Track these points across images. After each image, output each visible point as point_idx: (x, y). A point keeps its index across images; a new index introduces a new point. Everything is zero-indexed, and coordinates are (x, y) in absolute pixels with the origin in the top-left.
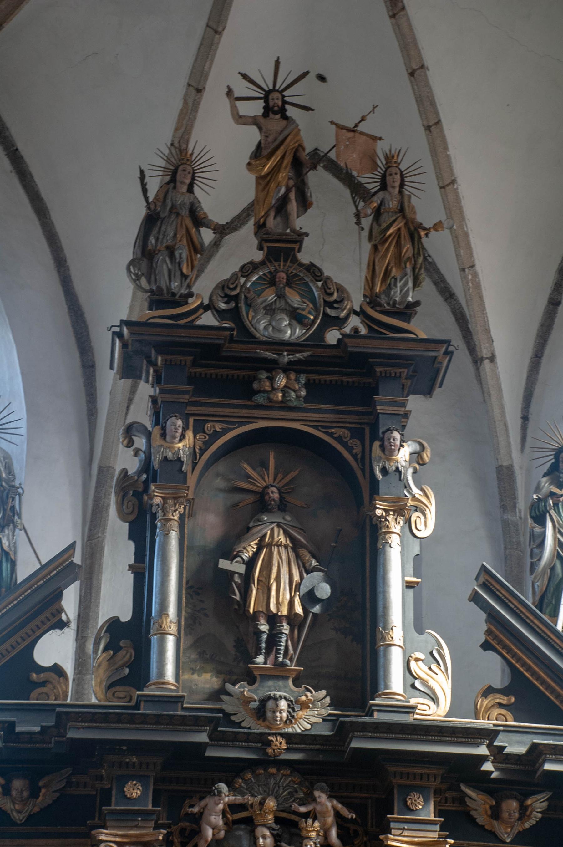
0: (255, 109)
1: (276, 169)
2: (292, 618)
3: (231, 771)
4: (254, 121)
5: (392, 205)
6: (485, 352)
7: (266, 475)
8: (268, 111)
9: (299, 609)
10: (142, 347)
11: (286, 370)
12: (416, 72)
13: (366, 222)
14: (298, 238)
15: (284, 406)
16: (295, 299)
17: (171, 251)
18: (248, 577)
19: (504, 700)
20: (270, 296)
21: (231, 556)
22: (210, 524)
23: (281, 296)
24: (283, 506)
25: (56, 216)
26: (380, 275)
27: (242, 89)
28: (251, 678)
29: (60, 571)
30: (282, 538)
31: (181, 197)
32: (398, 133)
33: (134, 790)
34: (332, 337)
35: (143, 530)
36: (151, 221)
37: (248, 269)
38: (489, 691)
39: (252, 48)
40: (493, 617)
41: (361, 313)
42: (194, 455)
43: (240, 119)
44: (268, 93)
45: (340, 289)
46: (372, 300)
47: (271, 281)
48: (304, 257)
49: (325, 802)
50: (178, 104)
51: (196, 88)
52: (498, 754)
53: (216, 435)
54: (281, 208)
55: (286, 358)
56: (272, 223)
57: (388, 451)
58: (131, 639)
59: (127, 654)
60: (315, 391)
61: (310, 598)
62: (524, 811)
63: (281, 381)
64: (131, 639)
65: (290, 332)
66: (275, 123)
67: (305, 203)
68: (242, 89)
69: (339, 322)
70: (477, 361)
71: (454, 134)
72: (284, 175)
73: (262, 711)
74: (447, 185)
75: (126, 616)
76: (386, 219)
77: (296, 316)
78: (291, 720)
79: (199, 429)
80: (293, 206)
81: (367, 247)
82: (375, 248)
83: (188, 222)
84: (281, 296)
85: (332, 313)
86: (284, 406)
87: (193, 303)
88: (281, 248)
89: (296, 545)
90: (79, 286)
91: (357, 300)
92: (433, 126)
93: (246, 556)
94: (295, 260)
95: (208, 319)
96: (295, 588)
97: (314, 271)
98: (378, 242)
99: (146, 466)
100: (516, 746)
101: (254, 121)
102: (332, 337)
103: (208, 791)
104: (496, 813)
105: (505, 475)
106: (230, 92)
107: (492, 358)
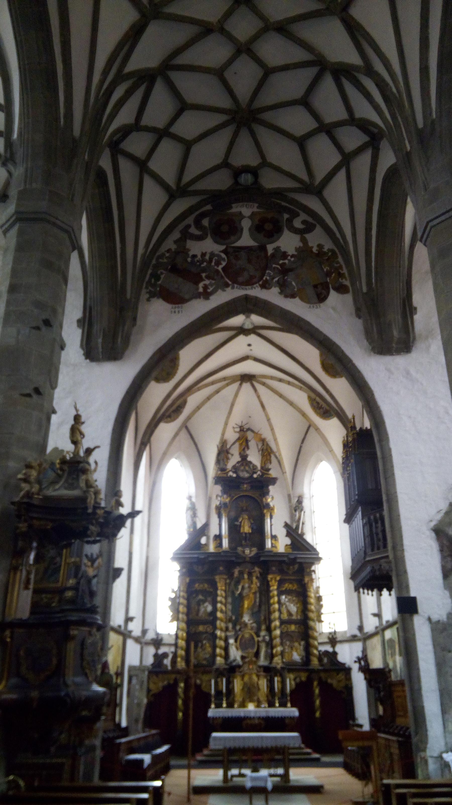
0: (238, 430)
1: (242, 443)
2: (249, 533)
3: (239, 564)
4: (238, 432)
5: (265, 448)
6: (284, 471)
7: (244, 503)
8: (241, 430)
9: (250, 531)
10: (218, 480)
11: (246, 483)
12: (269, 420)
13: (260, 452)
14: (247, 456)
15: (246, 491)
16: (247, 468)
17: (223, 460)
18: (240, 526)
19: (289, 547)
20: (242, 468)
21: (237, 521)
22: (233, 514)
23: (245, 468)
24: (246, 510)
25: (199, 446)
26: (263, 462)
27: (235, 426)
28: (241, 545)
29: (206, 526)
30: (247, 517)
31: (225, 449)
32: (266, 434)
33: (221, 568)
34: (255, 476)
35: (220, 517)
36: (219, 454)
37: (238, 462)
38: (287, 545)
39: (237, 418)
40: (287, 531)
41: (260, 471)
42: (230, 501)
43: (236, 432)
44: (241, 427)
45: (256, 466)
46: (262, 468)
47: (242, 465)
48: (249, 459)
49: (257, 569)
50: (223, 427)
51: (226, 424)
52: (289, 559)
53: (233, 497)
54: (244, 449)
55: (246, 481)
56: (242, 453)
57: (266, 500)
58: (218, 538)
59: (218, 542)
60: (252, 487)
61: (252, 529)
62: (294, 568)
63: (245, 486)
64: (218, 538)
65: (247, 475)
66: (242, 433)
67: (248, 448)
68: (235, 426)
69: (256, 473)
70: (283, 473)
71: (276, 430)
72: (244, 444)
73: (244, 552)
74: (275, 440)
75: (218, 533)
76: (264, 451)
77: (247, 472)
78: (250, 554)
79: (230, 496)
80: (246, 449)
81: (261, 457)
82: (262, 457)
83: (226, 454)
84: (245, 468)
85: (255, 471)
86: (246, 491)
87: (228, 470)
88: (244, 457)
89: (249, 519)
90: (203, 459)
91: (259, 468)
92: (272, 429)
93: (240, 521)
94: (247, 461)
95: (231, 474)
96: (250, 527)
97: (250, 462)
98: (263, 456)
99: (220, 504)
100: (292, 557)
101: (238, 432)
102: (255, 476)
103: (235, 568)
104: (288, 569)
105: (289, 496)
106: (234, 428)
107: (286, 473)
